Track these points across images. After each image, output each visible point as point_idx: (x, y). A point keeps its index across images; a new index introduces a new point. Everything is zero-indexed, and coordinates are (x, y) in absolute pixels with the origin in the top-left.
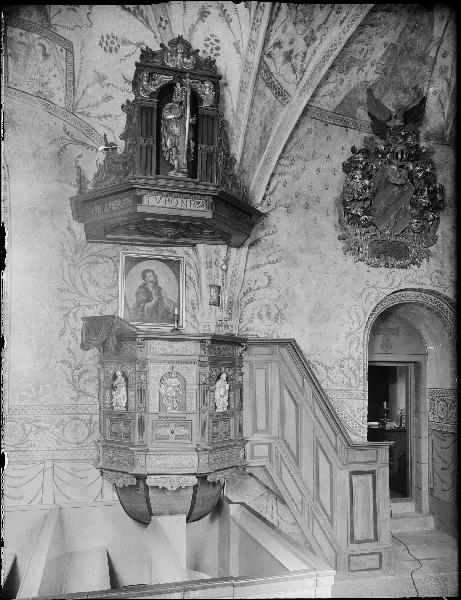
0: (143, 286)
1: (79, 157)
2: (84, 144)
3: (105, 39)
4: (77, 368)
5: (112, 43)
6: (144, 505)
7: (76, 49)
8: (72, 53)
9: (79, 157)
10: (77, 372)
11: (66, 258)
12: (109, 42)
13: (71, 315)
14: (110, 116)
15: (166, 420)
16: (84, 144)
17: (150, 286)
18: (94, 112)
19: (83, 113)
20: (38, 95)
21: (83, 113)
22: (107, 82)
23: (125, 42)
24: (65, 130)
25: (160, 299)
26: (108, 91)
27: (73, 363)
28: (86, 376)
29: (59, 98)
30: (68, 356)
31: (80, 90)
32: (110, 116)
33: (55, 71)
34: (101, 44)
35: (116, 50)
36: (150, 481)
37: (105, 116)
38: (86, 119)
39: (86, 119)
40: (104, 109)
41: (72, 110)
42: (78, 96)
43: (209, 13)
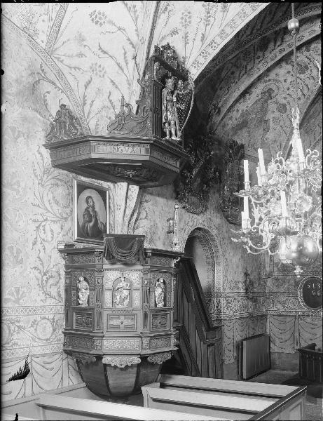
0: (87, 210)
1: (48, 92)
2: (53, 83)
3: (96, 13)
4: (45, 274)
5: (100, 18)
6: (103, 378)
9: (48, 92)
11: (37, 176)
12: (98, 16)
14: (79, 69)
15: (117, 314)
16: (53, 83)
17: (90, 209)
18: (67, 61)
19: (58, 59)
20: (25, 30)
21: (58, 59)
22: (85, 43)
23: (111, 22)
24: (41, 67)
25: (96, 220)
26: (83, 50)
28: (51, 281)
29: (42, 39)
30: (38, 264)
31: (61, 39)
32: (79, 69)
33: (46, 18)
35: (101, 25)
36: (106, 360)
37: (75, 68)
38: (59, 64)
40: (75, 62)
41: (49, 52)
42: (59, 44)
43: (178, 33)
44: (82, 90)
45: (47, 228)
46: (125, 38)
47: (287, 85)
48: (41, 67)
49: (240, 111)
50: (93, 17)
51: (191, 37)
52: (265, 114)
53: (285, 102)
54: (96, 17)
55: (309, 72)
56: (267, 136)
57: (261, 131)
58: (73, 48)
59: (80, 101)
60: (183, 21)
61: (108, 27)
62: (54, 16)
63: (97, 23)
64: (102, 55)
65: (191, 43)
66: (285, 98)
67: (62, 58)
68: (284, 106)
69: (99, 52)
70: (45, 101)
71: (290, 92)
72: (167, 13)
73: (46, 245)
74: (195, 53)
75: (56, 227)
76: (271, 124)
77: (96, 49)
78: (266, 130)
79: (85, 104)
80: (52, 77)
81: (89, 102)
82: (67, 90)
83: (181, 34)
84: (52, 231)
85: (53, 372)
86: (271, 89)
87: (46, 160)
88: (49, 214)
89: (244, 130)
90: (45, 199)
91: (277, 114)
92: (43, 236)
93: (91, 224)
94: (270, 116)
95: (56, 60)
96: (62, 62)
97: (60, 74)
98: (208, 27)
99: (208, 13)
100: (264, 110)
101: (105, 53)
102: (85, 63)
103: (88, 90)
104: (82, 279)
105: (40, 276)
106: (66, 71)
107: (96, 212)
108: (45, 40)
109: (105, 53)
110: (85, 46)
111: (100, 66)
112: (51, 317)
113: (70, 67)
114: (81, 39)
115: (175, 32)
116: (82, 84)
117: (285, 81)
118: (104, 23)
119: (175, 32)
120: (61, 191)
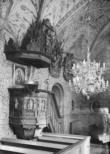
0: (18, 75)
1: (5, 33)
3: (23, 6)
4: (3, 97)
5: (24, 8)
7: (14, 4)
8: (12, 5)
9: (5, 33)
10: (3, 98)
12: (24, 7)
13: (2, 81)
16: (7, 30)
17: (19, 75)
19: (9, 21)
21: (9, 21)
22: (19, 16)
23: (28, 9)
24: (3, 24)
25: (21, 79)
26: (19, 19)
27: (2, 96)
28: (5, 100)
31: (10, 15)
33: (5, 7)
34: (21, 7)
35: (24, 10)
37: (15, 25)
38: (9, 23)
39: (9, 23)
40: (16, 23)
41: (6, 19)
42: (9, 16)
43: (51, 14)
44: (17, 33)
45: (4, 81)
46: (33, 15)
48: (3, 24)
49: (72, 42)
50: (22, 7)
51: (56, 16)
52: (81, 43)
53: (87, 39)
54: (23, 7)
55: (97, 29)
57: (80, 49)
58: (15, 18)
59: (16, 37)
60: (53, 10)
61: (27, 11)
62: (8, 6)
63: (23, 9)
64: (25, 21)
65: (56, 18)
67: (11, 21)
69: (24, 20)
70: (4, 36)
72: (48, 7)
73: (4, 87)
74: (57, 22)
75: (7, 81)
76: (83, 47)
77: (22, 19)
78: (82, 49)
79: (18, 38)
80: (7, 28)
81: (19, 37)
82: (12, 33)
83: (52, 15)
84: (6, 82)
85: (5, 131)
86: (83, 35)
87: (4, 57)
88: (5, 76)
89: (74, 48)
90: (4, 71)
91: (85, 43)
92: (3, 84)
93: (19, 80)
94: (83, 44)
95: (8, 22)
96: (10, 22)
97: (10, 27)
98: (62, 13)
99: (62, 8)
100: (81, 42)
101: (26, 20)
102: (18, 23)
103: (20, 33)
104: (16, 99)
105: (1, 98)
106: (12, 26)
107: (21, 76)
108: (5, 15)
109: (26, 20)
110: (19, 17)
111: (24, 25)
112: (5, 112)
113: (13, 25)
114: (17, 15)
115: (50, 14)
116: (17, 31)
118: (26, 9)
119: (50, 14)
120: (10, 68)
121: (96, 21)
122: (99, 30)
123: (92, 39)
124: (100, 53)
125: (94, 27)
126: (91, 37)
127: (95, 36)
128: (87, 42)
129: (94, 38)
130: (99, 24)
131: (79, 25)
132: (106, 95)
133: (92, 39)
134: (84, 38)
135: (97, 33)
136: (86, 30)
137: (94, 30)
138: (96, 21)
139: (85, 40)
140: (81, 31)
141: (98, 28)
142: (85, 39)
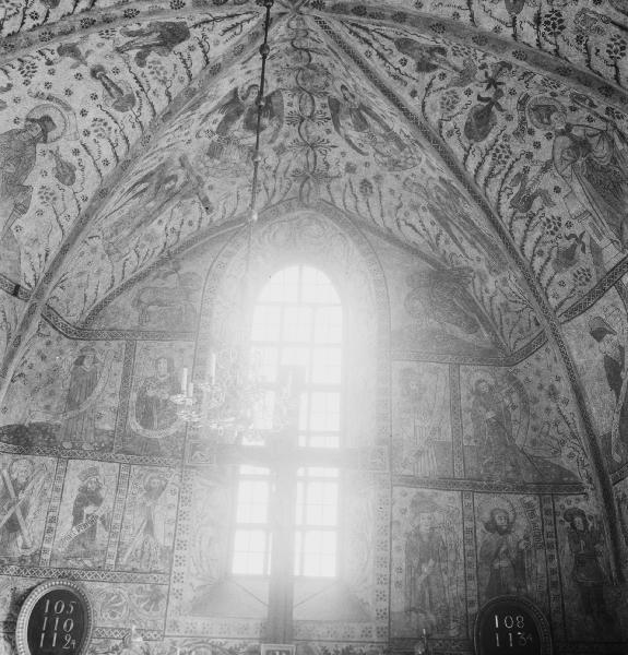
47: (86, 123)
52: (27, 170)
53: (74, 160)
55: (135, 109)
56: (19, 222)
66: (76, 152)
68: (71, 169)
71: (88, 141)
76: (36, 201)
78: (21, 209)
86: (47, 119)
91: (51, 181)
94: (35, 180)
117: (84, 113)
121: (141, 60)
122: (146, 117)
123: (101, 167)
124: (130, 283)
125: (119, 90)
126: (95, 152)
127: (121, 152)
128: (66, 174)
129: (112, 161)
130: (155, 85)
131: (30, 23)
132: (139, 541)
133: (100, 162)
134: (53, 147)
135: (134, 135)
136: (68, 92)
137: (119, 115)
138: (141, 60)
139: (53, 164)
140: (42, 89)
141: (146, 109)
142: (55, 154)
